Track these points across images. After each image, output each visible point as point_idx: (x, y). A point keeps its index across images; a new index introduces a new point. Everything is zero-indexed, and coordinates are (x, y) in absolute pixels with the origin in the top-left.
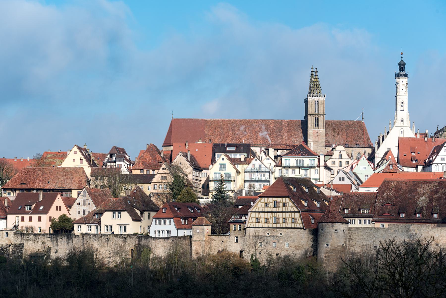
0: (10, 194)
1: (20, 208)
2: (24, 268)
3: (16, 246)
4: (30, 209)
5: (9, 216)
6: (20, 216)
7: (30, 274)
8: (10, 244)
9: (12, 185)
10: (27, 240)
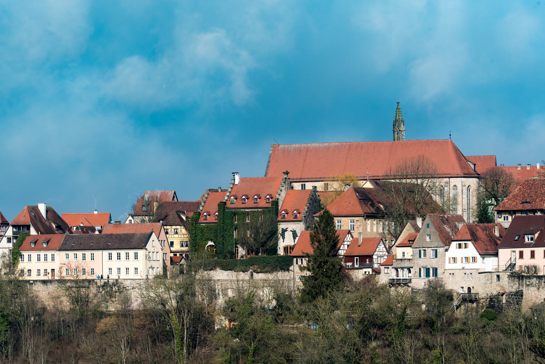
0: (507, 219)
1: (516, 239)
2: (521, 327)
3: (512, 295)
4: (532, 239)
5: (501, 251)
6: (518, 250)
7: (531, 336)
8: (503, 292)
9: (510, 204)
10: (528, 285)
